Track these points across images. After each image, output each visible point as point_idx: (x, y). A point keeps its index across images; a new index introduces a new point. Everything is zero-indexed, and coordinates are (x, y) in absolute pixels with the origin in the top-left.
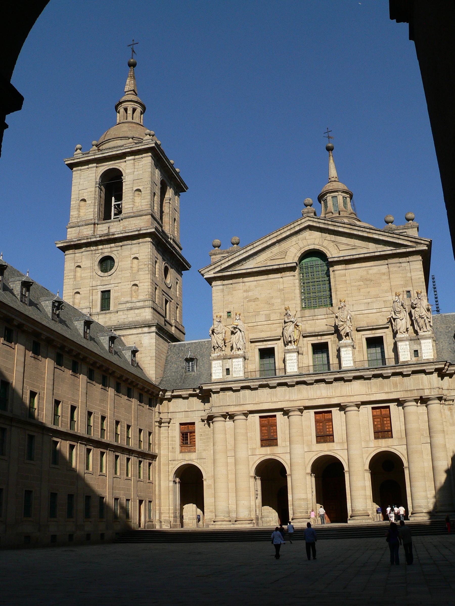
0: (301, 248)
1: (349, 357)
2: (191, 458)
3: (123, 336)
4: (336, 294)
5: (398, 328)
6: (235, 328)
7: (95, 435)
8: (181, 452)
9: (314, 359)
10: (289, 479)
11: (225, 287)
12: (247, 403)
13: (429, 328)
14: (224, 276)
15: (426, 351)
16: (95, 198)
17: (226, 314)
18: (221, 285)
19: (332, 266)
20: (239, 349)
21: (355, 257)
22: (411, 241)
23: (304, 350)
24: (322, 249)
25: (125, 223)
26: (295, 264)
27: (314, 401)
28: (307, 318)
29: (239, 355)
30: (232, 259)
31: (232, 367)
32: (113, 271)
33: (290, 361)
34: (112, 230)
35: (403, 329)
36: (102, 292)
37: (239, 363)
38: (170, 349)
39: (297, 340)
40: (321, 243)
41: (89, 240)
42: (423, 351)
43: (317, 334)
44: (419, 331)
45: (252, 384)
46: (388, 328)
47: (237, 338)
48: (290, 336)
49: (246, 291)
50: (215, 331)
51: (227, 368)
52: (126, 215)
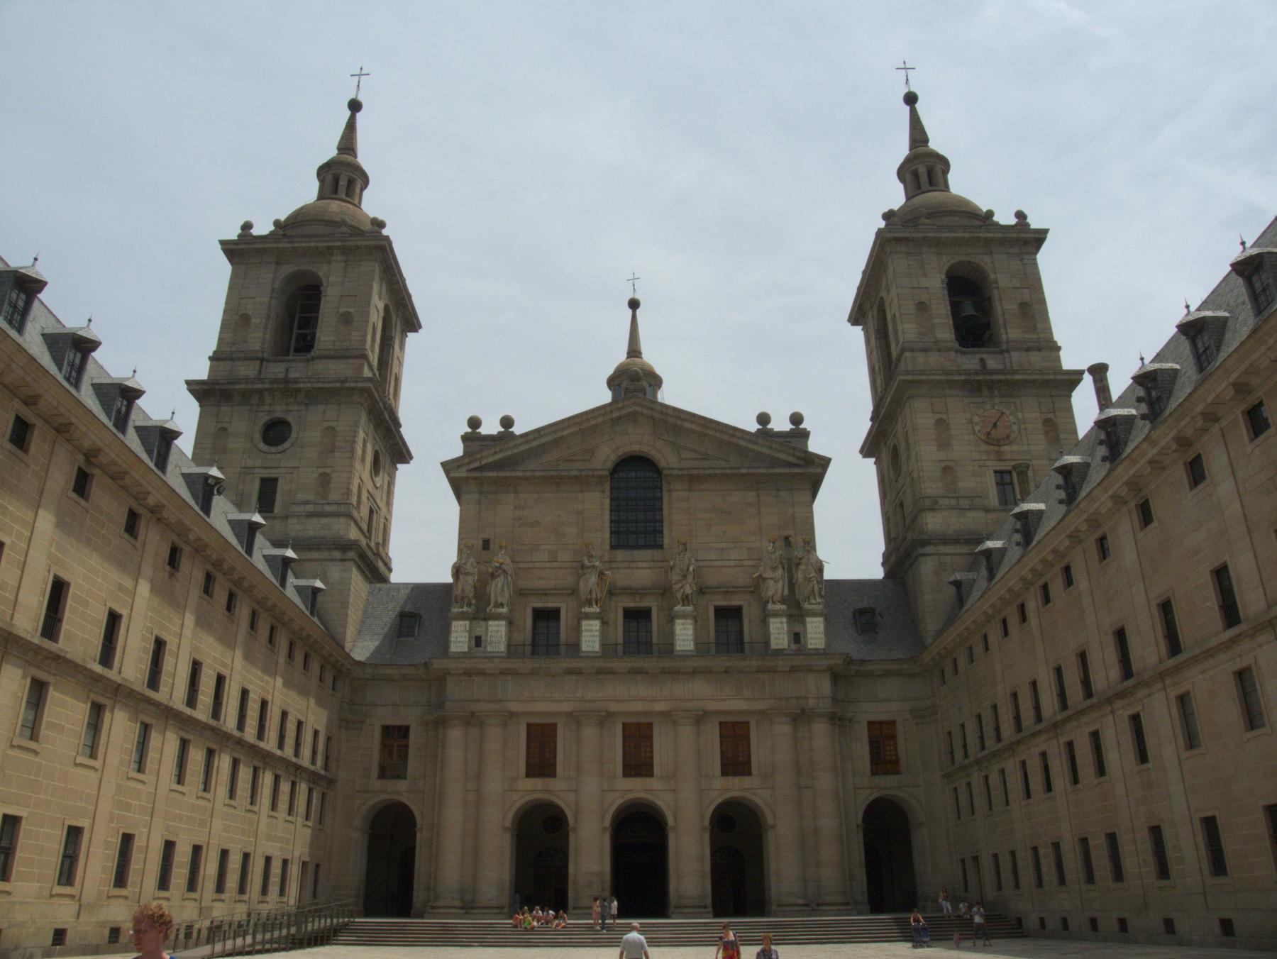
2: (399, 790)
5: (770, 593)
6: (500, 568)
7: (250, 734)
8: (379, 778)
9: (626, 631)
10: (572, 837)
16: (268, 316)
17: (481, 543)
19: (669, 483)
20: (502, 605)
21: (707, 472)
22: (798, 458)
25: (319, 366)
30: (501, 451)
32: (286, 445)
34: (292, 375)
35: (778, 597)
36: (263, 480)
38: (370, 593)
41: (250, 386)
47: (500, 585)
49: (517, 507)
51: (478, 634)
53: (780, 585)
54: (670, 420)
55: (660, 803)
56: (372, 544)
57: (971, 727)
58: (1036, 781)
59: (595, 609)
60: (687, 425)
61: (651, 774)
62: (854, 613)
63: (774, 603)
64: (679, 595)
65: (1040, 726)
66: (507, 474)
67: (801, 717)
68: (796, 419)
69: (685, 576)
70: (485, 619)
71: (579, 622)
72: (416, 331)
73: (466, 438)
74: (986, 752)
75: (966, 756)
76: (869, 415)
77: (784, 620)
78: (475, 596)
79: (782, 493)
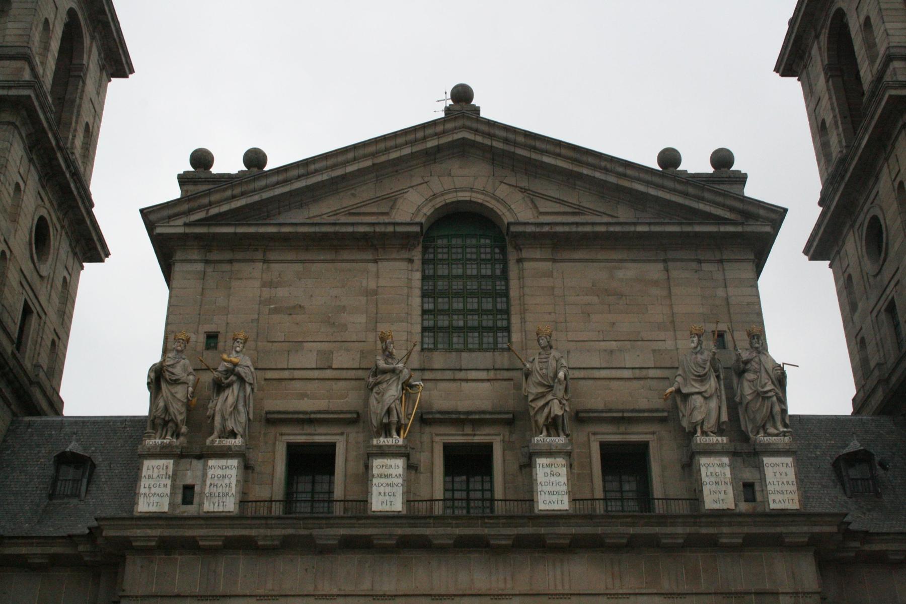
0: (435, 196)
1: (558, 484)
4: (523, 321)
5: (698, 417)
6: (230, 372)
11: (210, 269)
12: (239, 591)
13: (782, 429)
14: (215, 234)
15: (778, 488)
17: (202, 338)
18: (201, 261)
19: (518, 248)
20: (233, 434)
21: (581, 229)
23: (422, 458)
24: (492, 204)
26: (417, 229)
28: (438, 375)
29: (229, 448)
30: (243, 194)
31: (204, 481)
33: (383, 481)
37: (228, 472)
39: (406, 425)
40: (489, 189)
42: (770, 488)
43: (462, 417)
44: (751, 436)
45: (262, 532)
46: (663, 420)
47: (231, 400)
49: (269, 284)
50: (167, 375)
51: (189, 481)
53: (713, 404)
54: (520, 151)
56: (28, 365)
59: (397, 440)
60: (546, 159)
62: (836, 465)
63: (704, 433)
64: (541, 419)
66: (252, 230)
68: (722, 159)
69: (551, 387)
70: (200, 457)
71: (367, 467)
72: (125, 76)
73: (184, 180)
76: (818, 197)
78: (188, 421)
79: (706, 267)
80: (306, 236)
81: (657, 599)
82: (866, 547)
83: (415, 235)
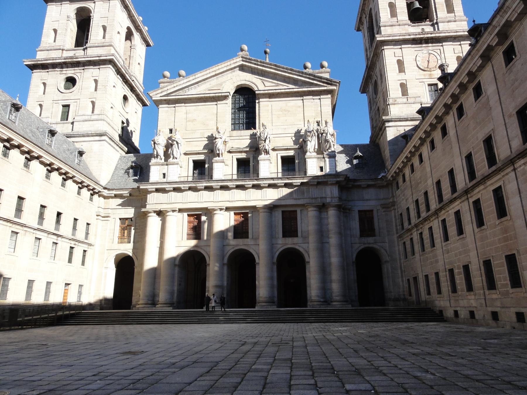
3: (77, 142)
19: (259, 99)
20: (176, 158)
27: (234, 202)
35: (312, 150)
40: (251, 80)
48: (219, 150)
50: (157, 142)
52: (92, 45)
55: (251, 251)
57: (412, 207)
58: (452, 230)
59: (221, 158)
61: (247, 237)
65: (455, 195)
67: (322, 208)
70: (167, 165)
74: (421, 219)
75: (410, 223)
77: (315, 160)
80: (196, 98)
81: (292, 200)
82: (356, 184)
83: (228, 96)
